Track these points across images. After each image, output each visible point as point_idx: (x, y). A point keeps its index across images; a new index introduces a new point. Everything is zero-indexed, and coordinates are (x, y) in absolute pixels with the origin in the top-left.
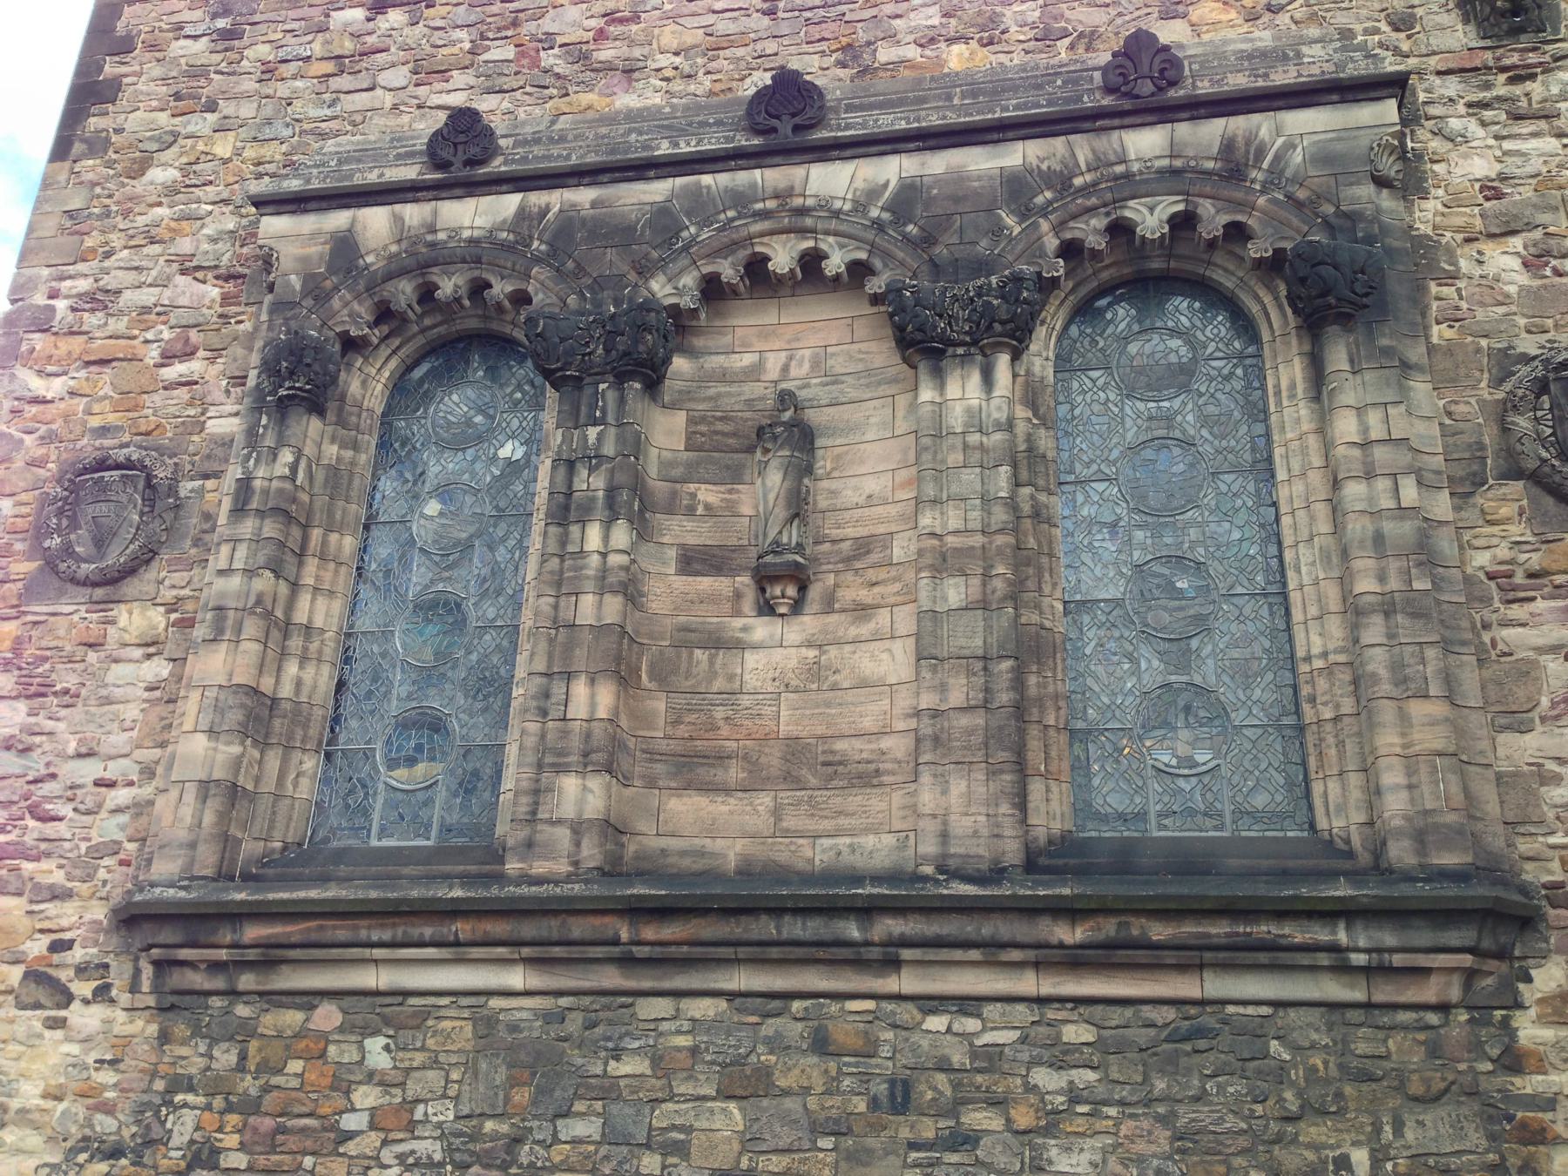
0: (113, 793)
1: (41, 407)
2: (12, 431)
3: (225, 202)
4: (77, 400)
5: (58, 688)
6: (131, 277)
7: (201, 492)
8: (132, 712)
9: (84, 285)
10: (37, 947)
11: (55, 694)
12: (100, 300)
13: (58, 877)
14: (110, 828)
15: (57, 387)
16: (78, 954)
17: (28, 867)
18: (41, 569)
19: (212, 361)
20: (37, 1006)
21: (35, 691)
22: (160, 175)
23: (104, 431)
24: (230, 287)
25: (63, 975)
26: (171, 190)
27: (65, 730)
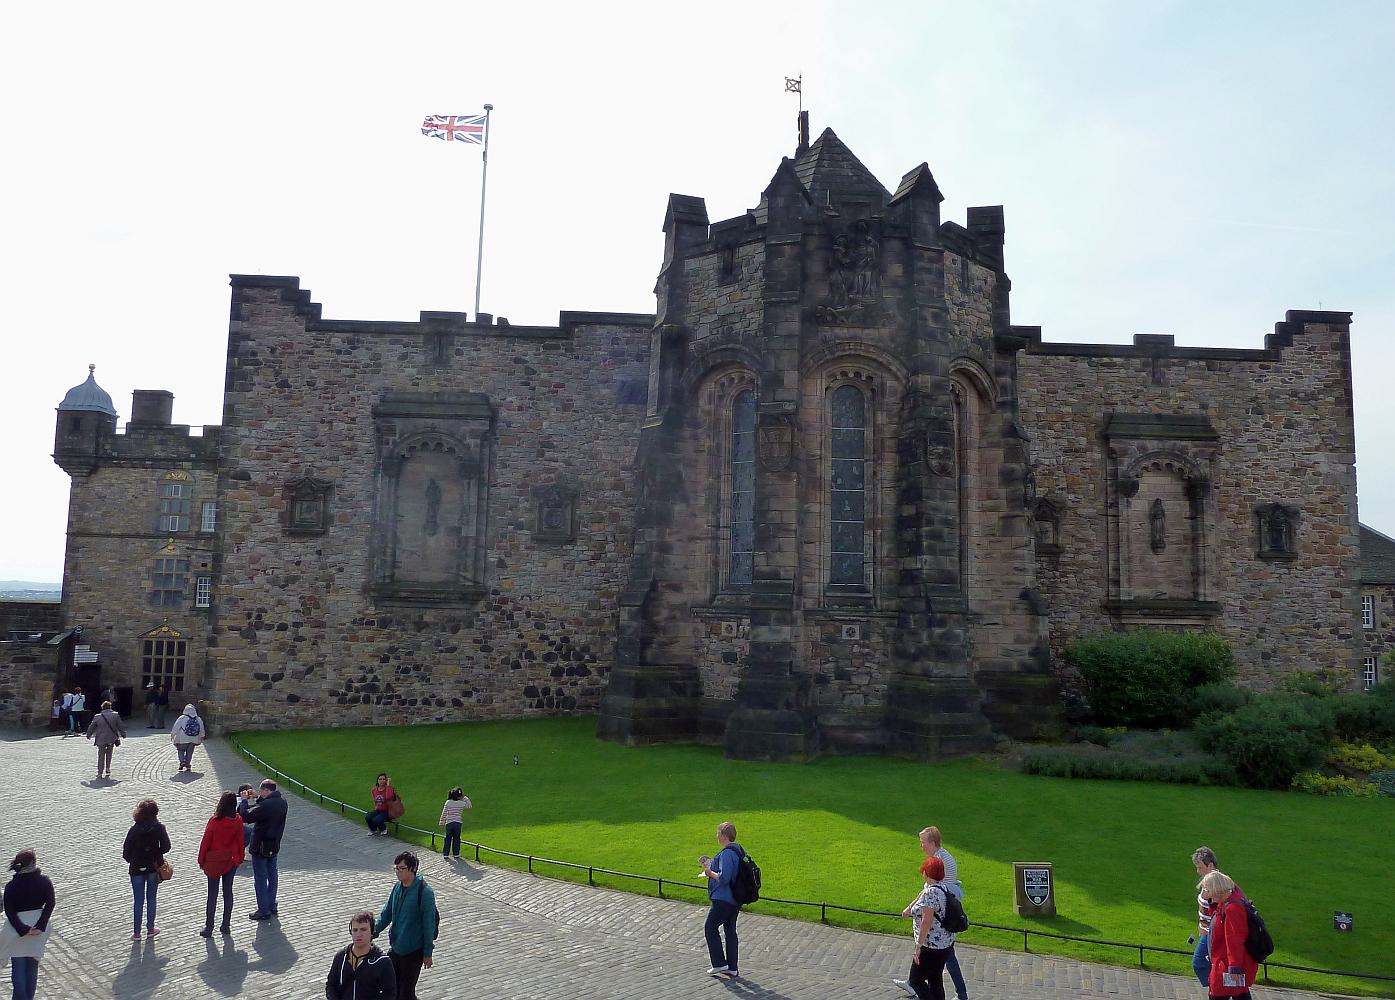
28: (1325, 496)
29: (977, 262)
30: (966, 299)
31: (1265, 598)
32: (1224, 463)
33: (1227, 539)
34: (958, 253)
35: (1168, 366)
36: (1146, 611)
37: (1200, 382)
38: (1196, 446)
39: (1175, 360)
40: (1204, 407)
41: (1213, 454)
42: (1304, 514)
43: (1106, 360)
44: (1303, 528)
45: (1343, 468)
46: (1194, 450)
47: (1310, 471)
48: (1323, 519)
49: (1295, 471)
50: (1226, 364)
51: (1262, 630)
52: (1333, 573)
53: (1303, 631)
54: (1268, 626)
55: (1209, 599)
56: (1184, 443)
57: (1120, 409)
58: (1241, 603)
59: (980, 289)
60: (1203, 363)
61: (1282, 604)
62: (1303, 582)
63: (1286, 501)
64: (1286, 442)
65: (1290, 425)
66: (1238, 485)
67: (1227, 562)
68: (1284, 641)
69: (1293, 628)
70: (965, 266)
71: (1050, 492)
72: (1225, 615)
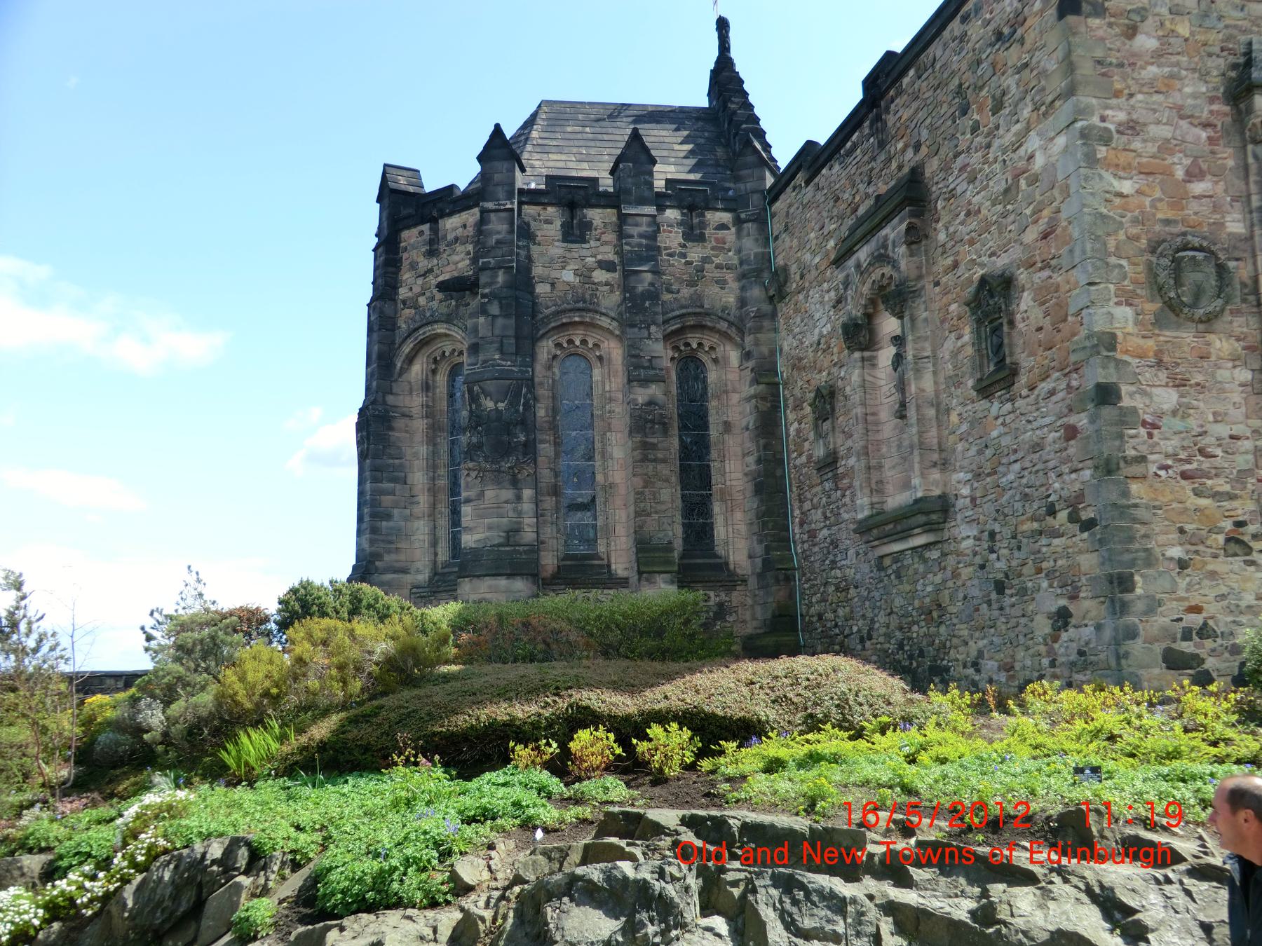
0: (1239, 443)
1: (1124, 200)
2: (1111, 214)
3: (1194, 70)
4: (1142, 198)
5: (1193, 382)
6: (1151, 117)
7: (1237, 268)
8: (1237, 397)
9: (1122, 116)
10: (1228, 525)
11: (1191, 386)
12: (1132, 128)
13: (1227, 488)
14: (1244, 461)
15: (1127, 187)
16: (1252, 528)
17: (1209, 482)
18: (1162, 310)
19: (1216, 183)
20: (1236, 555)
21: (1180, 383)
22: (1146, 42)
23: (1167, 222)
24: (1210, 132)
25: (1246, 539)
26: (1158, 56)
27: (1205, 406)
28: (1042, 225)
29: (450, 215)
30: (435, 261)
31: (994, 472)
32: (942, 237)
33: (952, 373)
34: (423, 223)
35: (887, 110)
36: (875, 531)
37: (915, 105)
38: (894, 229)
39: (892, 93)
40: (917, 147)
41: (910, 229)
42: (1022, 276)
43: (849, 144)
44: (1023, 307)
45: (1061, 141)
46: (892, 236)
47: (1023, 183)
48: (1046, 273)
49: (1007, 191)
50: (931, 50)
51: (992, 535)
52: (1064, 386)
53: (1036, 525)
54: (997, 528)
55: (920, 495)
56: (883, 232)
57: (862, 211)
58: (973, 489)
59: (457, 239)
60: (912, 72)
61: (1011, 477)
62: (1029, 422)
63: (1001, 262)
64: (996, 143)
65: (997, 107)
66: (956, 265)
67: (954, 418)
68: (1016, 554)
69: (1022, 523)
70: (435, 230)
71: (829, 374)
72: (959, 517)
